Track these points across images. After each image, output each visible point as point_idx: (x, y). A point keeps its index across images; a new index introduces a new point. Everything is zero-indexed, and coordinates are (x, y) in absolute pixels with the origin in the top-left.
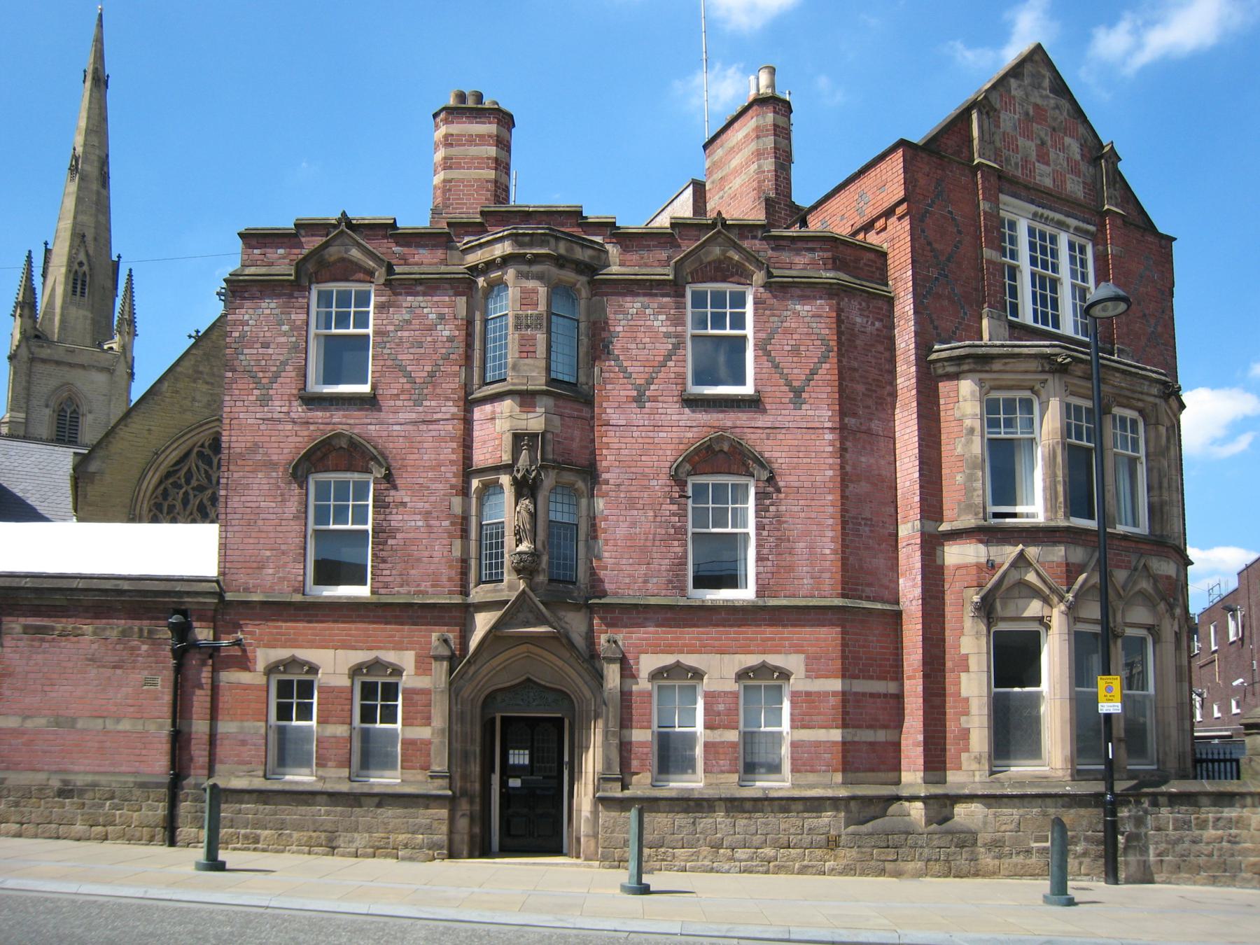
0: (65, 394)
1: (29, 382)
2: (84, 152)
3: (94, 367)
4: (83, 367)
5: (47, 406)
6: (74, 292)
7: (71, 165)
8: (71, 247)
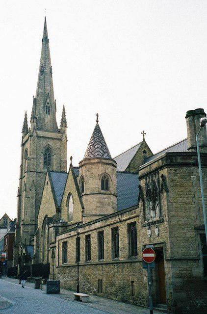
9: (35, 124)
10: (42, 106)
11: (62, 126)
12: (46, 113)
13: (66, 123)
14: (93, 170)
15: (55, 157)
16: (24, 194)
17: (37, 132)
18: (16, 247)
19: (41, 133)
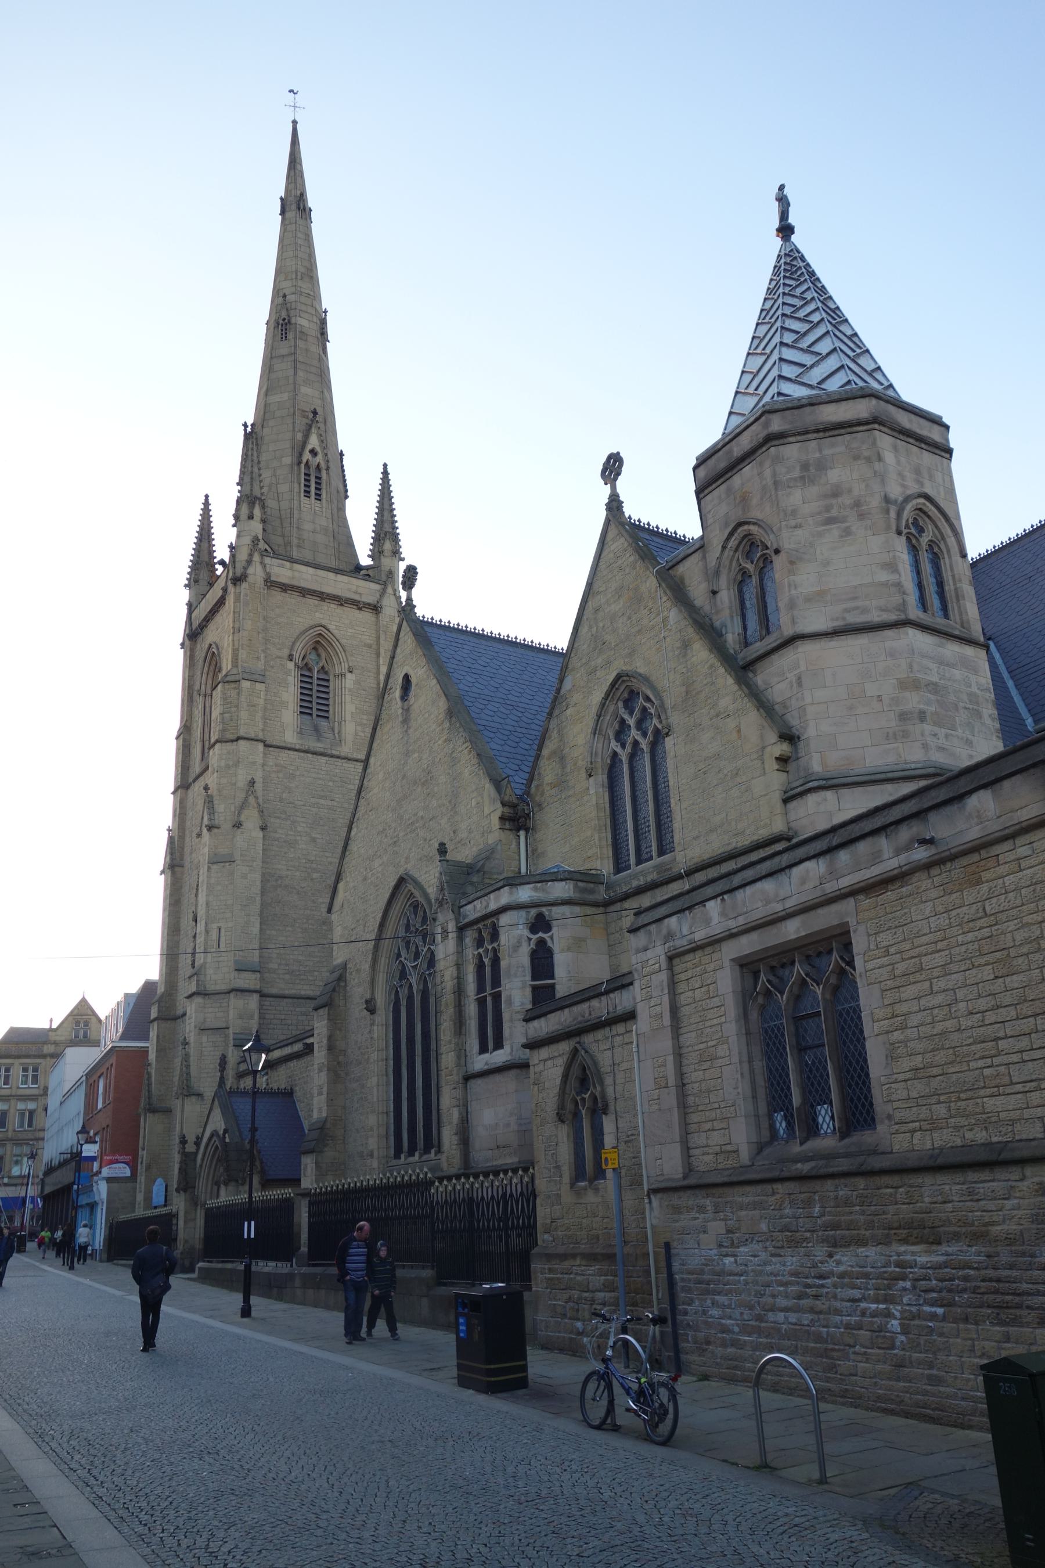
9: (256, 527)
10: (287, 460)
11: (377, 552)
12: (307, 493)
13: (395, 538)
14: (834, 475)
15: (350, 680)
16: (203, 848)
17: (267, 560)
18: (152, 1110)
19: (283, 572)
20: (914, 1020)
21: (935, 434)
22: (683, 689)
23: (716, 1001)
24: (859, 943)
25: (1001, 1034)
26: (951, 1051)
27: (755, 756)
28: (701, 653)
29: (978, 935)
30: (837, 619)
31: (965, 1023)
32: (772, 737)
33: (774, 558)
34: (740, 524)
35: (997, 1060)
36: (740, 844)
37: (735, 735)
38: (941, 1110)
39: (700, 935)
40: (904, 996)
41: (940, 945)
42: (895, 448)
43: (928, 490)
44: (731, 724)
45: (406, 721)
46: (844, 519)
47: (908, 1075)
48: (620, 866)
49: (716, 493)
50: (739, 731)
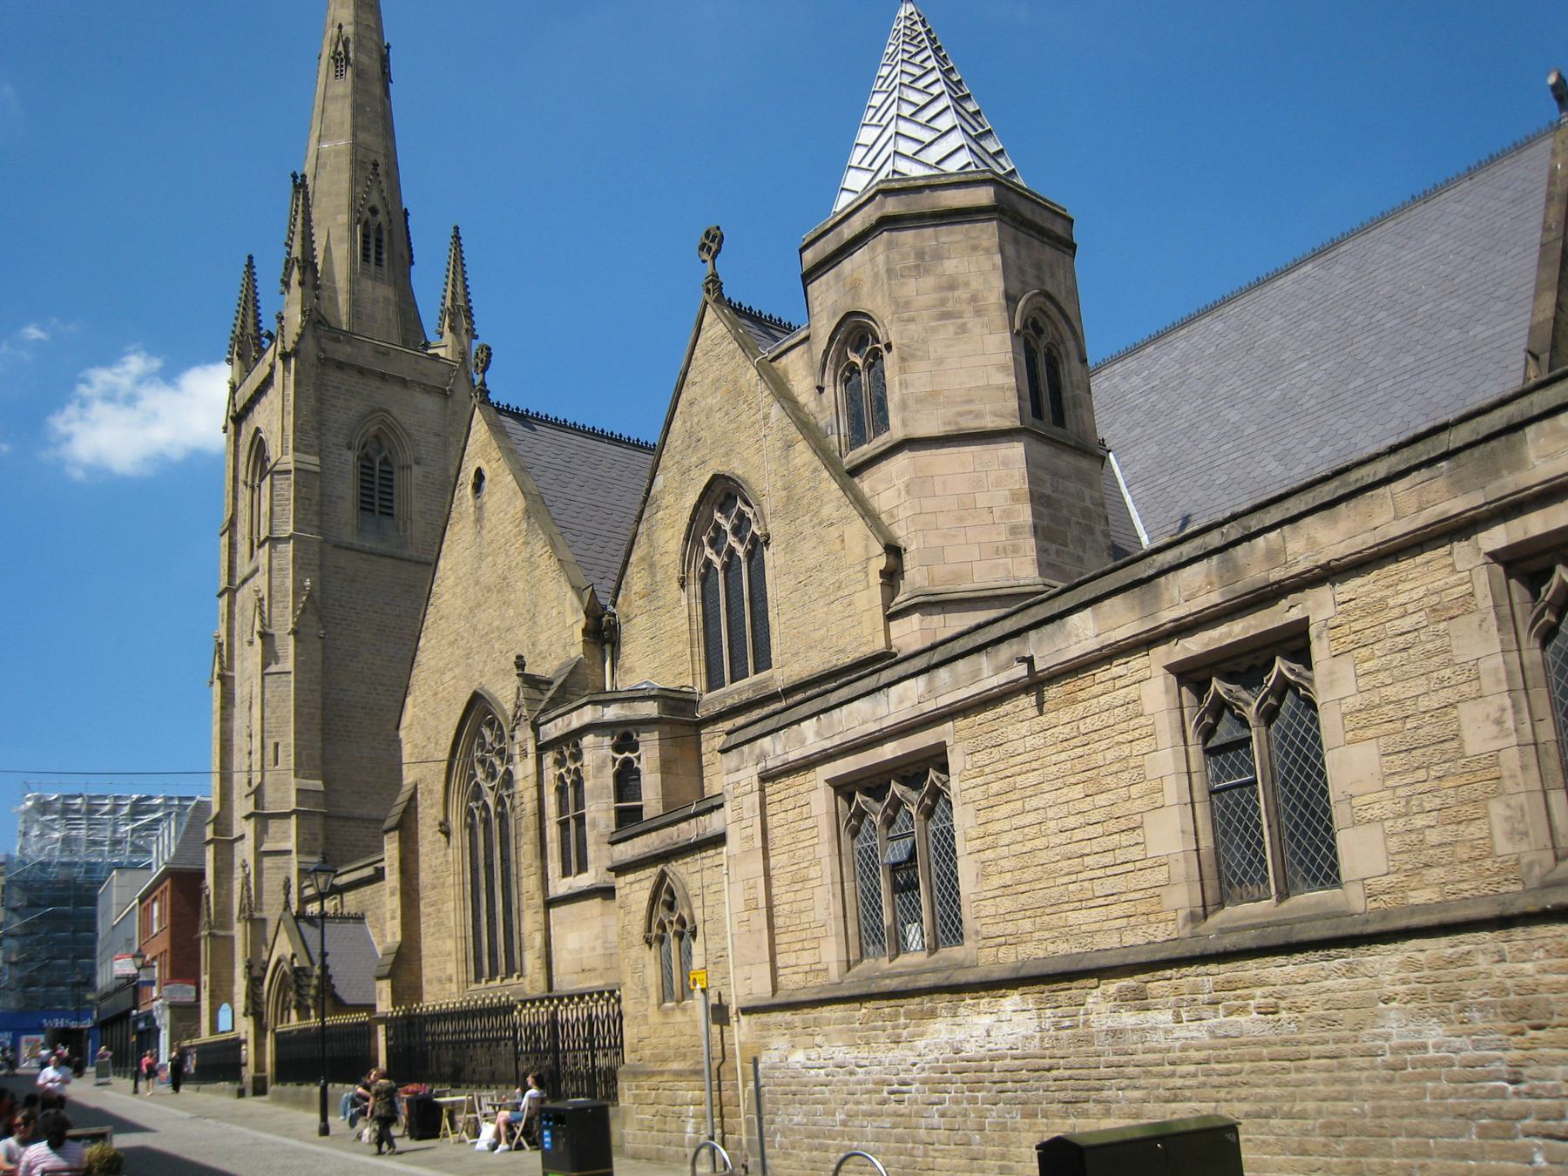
0: (373, 430)
1: (320, 400)
2: (357, 34)
3: (420, 384)
4: (403, 382)
5: (349, 447)
6: (366, 257)
7: (336, 52)
8: (354, 181)
14: (951, 266)
20: (1005, 839)
21: (1059, 228)
22: (784, 493)
23: (809, 823)
24: (955, 761)
25: (1087, 851)
26: (1039, 868)
27: (859, 568)
28: (803, 454)
29: (1072, 754)
30: (949, 424)
31: (1055, 840)
32: (878, 549)
33: (885, 353)
34: (849, 315)
35: (1081, 877)
36: (840, 662)
37: (837, 546)
38: (1027, 925)
39: (794, 755)
40: (997, 815)
41: (1035, 765)
42: (1016, 241)
43: (1049, 288)
44: (834, 532)
45: (479, 520)
46: (959, 315)
47: (997, 893)
48: (714, 682)
49: (823, 278)
50: (843, 541)
